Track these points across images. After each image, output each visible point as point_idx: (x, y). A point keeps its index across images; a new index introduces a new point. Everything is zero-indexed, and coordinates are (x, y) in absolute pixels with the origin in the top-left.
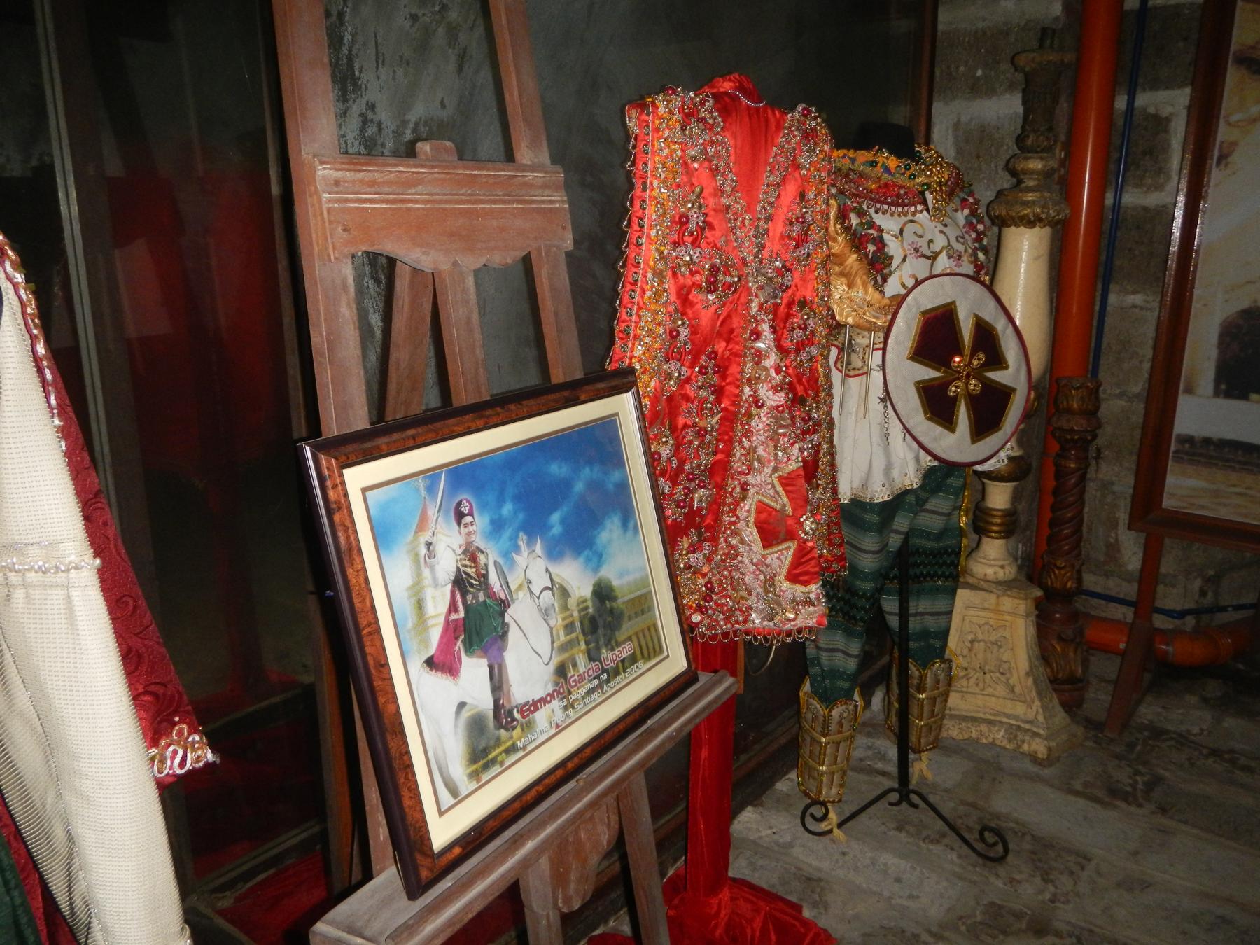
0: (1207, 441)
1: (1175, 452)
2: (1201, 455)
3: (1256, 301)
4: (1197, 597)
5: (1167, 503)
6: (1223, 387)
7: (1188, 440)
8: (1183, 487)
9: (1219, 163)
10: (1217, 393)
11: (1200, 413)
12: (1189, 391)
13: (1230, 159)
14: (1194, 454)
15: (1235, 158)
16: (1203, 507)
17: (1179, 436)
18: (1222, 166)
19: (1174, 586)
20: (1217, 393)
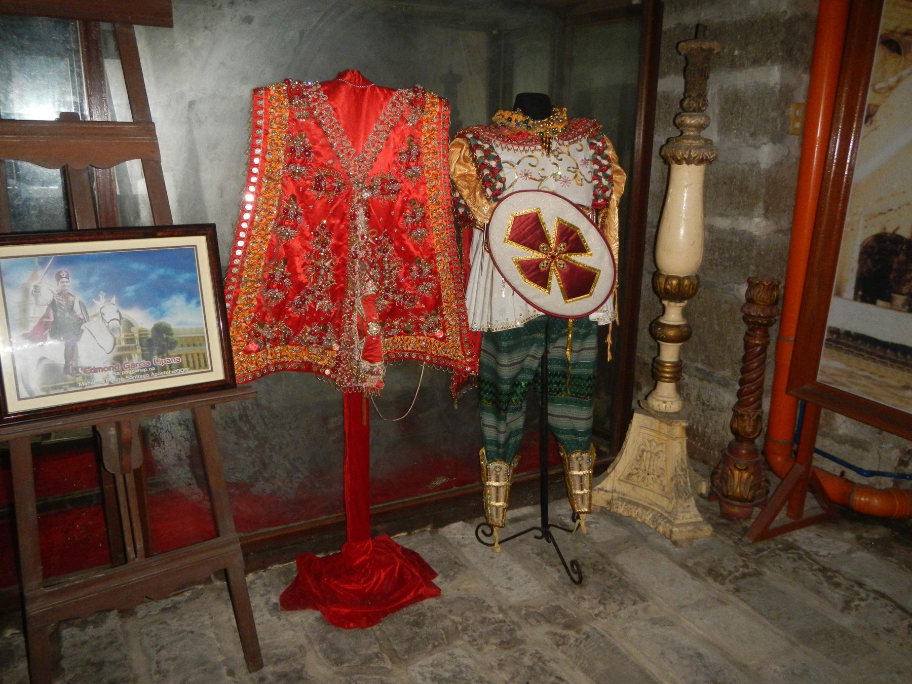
0: (848, 334)
1: (827, 340)
2: (842, 344)
3: (884, 229)
4: (896, 464)
5: (820, 378)
6: (860, 293)
7: (835, 331)
8: (832, 367)
9: (866, 121)
10: (855, 299)
11: (846, 313)
12: (839, 294)
13: (874, 118)
14: (838, 343)
15: (878, 117)
16: (842, 384)
17: (830, 327)
18: (868, 124)
19: (868, 451)
20: (855, 299)
